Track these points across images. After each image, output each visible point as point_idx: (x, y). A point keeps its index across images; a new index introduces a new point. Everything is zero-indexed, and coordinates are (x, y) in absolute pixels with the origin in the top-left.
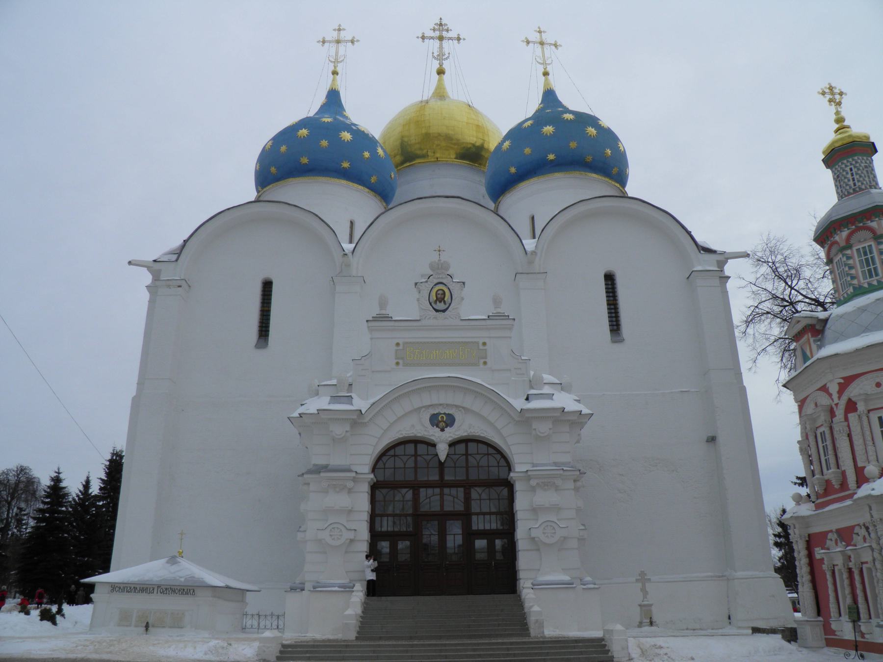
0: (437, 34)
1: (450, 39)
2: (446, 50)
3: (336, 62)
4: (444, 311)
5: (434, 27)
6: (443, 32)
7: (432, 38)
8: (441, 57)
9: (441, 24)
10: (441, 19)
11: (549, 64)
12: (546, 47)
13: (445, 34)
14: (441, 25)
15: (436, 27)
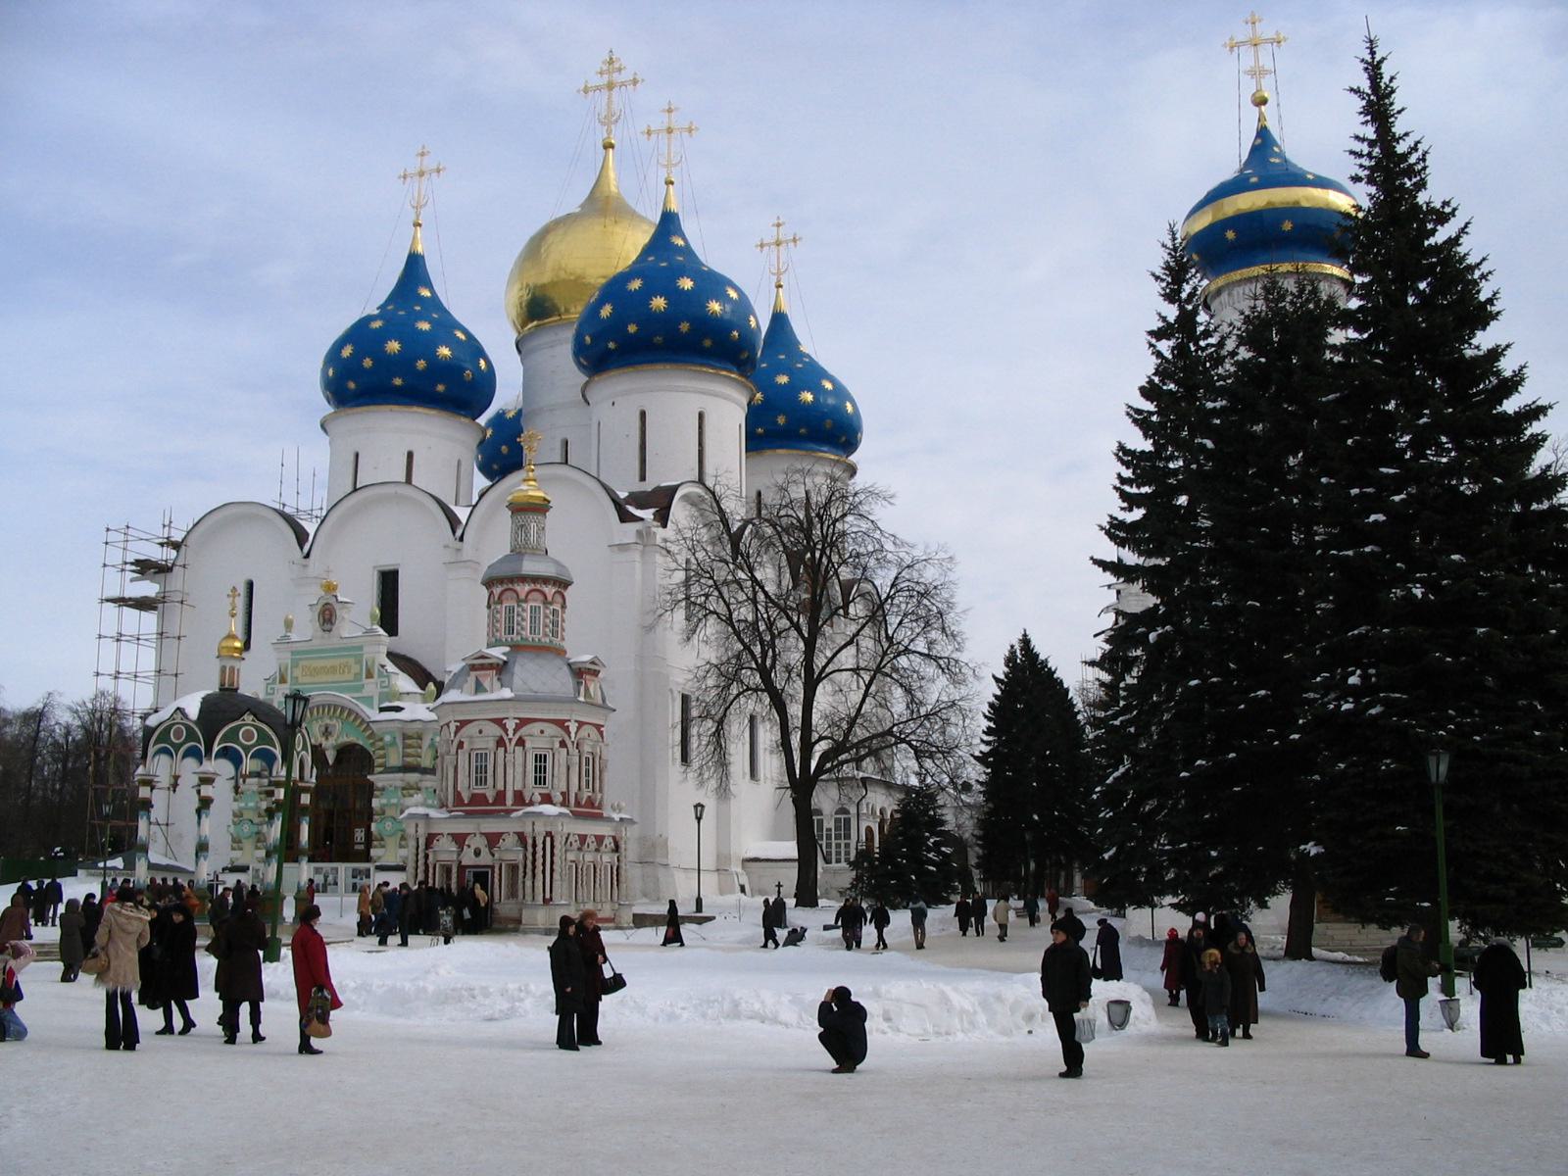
0: (605, 79)
1: (623, 84)
2: (615, 107)
3: (417, 208)
4: (330, 631)
5: (601, 68)
6: (614, 75)
7: (598, 88)
8: (609, 120)
9: (611, 59)
10: (611, 51)
11: (676, 165)
12: (676, 134)
13: (617, 78)
14: (611, 61)
15: (605, 68)
